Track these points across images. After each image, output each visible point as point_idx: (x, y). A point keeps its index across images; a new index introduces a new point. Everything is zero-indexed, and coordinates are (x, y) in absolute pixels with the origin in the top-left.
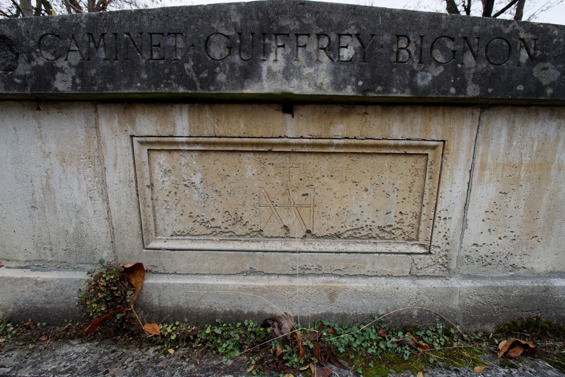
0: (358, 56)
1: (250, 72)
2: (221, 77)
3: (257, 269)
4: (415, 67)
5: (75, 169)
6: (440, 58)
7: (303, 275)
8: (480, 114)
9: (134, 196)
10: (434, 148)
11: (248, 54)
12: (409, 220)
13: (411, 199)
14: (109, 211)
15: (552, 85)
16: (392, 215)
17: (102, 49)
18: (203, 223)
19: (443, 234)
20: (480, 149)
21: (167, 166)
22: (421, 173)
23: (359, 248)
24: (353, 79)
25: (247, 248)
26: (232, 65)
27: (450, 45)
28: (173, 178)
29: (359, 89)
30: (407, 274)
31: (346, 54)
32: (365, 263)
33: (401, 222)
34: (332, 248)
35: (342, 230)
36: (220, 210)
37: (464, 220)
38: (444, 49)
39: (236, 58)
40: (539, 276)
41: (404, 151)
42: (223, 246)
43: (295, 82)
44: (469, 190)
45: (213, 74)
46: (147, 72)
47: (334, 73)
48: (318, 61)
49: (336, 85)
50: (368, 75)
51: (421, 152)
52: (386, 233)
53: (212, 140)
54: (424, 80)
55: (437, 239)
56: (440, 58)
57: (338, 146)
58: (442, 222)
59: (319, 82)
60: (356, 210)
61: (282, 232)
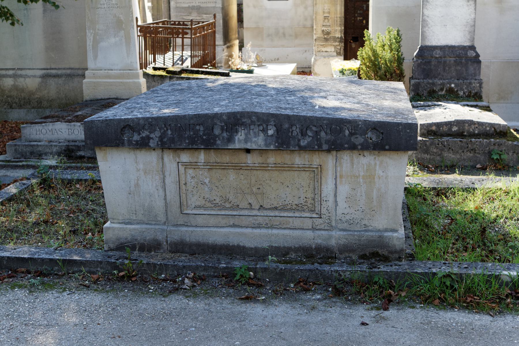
0: (275, 133)
1: (230, 140)
2: (219, 142)
3: (236, 223)
4: (300, 137)
5: (151, 177)
7: (259, 227)
9: (178, 189)
10: (317, 168)
11: (229, 133)
12: (310, 201)
13: (310, 191)
14: (165, 195)
15: (360, 144)
16: (302, 198)
17: (169, 131)
18: (210, 201)
19: (326, 208)
20: (339, 169)
22: (313, 179)
23: (286, 214)
24: (274, 143)
25: (231, 214)
26: (223, 137)
27: (314, 129)
28: (196, 180)
29: (276, 147)
30: (310, 227)
31: (270, 132)
32: (289, 222)
34: (272, 214)
35: (278, 206)
36: (218, 195)
37: (336, 201)
38: (311, 130)
40: (379, 231)
41: (303, 169)
42: (219, 213)
43: (249, 144)
44: (336, 187)
45: (216, 141)
46: (188, 140)
47: (266, 140)
48: (259, 136)
49: (266, 145)
50: (280, 141)
51: (311, 169)
52: (299, 208)
53: (215, 164)
54: (303, 143)
55: (324, 211)
57: (271, 167)
58: (325, 202)
59: (259, 144)
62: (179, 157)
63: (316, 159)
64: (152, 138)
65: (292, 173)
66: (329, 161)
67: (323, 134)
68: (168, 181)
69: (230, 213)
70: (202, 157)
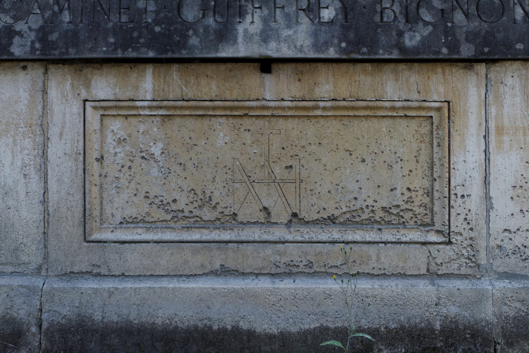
0: (340, 17)
1: (225, 34)
2: (194, 41)
3: (230, 264)
4: (401, 26)
5: (11, 140)
6: (428, 18)
7: (289, 274)
8: (487, 71)
9: (81, 172)
10: (439, 109)
11: (222, 16)
12: (420, 198)
13: (420, 171)
14: (46, 191)
16: (398, 192)
17: (66, 13)
18: (162, 205)
19: (463, 216)
20: (493, 110)
21: (122, 134)
22: (427, 139)
23: (358, 236)
24: (336, 41)
25: (217, 238)
26: (206, 29)
28: (128, 148)
29: (343, 51)
30: (423, 271)
31: (327, 14)
32: (369, 257)
33: (410, 201)
34: (324, 237)
35: (337, 213)
36: (185, 187)
37: (488, 198)
39: (210, 21)
41: (403, 113)
42: (186, 236)
43: (273, 45)
44: (487, 159)
45: (186, 37)
46: (114, 36)
47: (315, 35)
49: (316, 46)
50: (352, 36)
51: (423, 113)
52: (392, 217)
53: (179, 103)
54: (412, 40)
56: (428, 18)
57: (324, 108)
58: (460, 201)
59: (299, 44)
60: (353, 186)
61: (261, 217)
62: (88, 86)
63: (437, 85)
64: (20, 34)
65: (375, 124)
66: (469, 90)
67: (459, 17)
68: (55, 150)
69: (215, 235)
70: (147, 84)
